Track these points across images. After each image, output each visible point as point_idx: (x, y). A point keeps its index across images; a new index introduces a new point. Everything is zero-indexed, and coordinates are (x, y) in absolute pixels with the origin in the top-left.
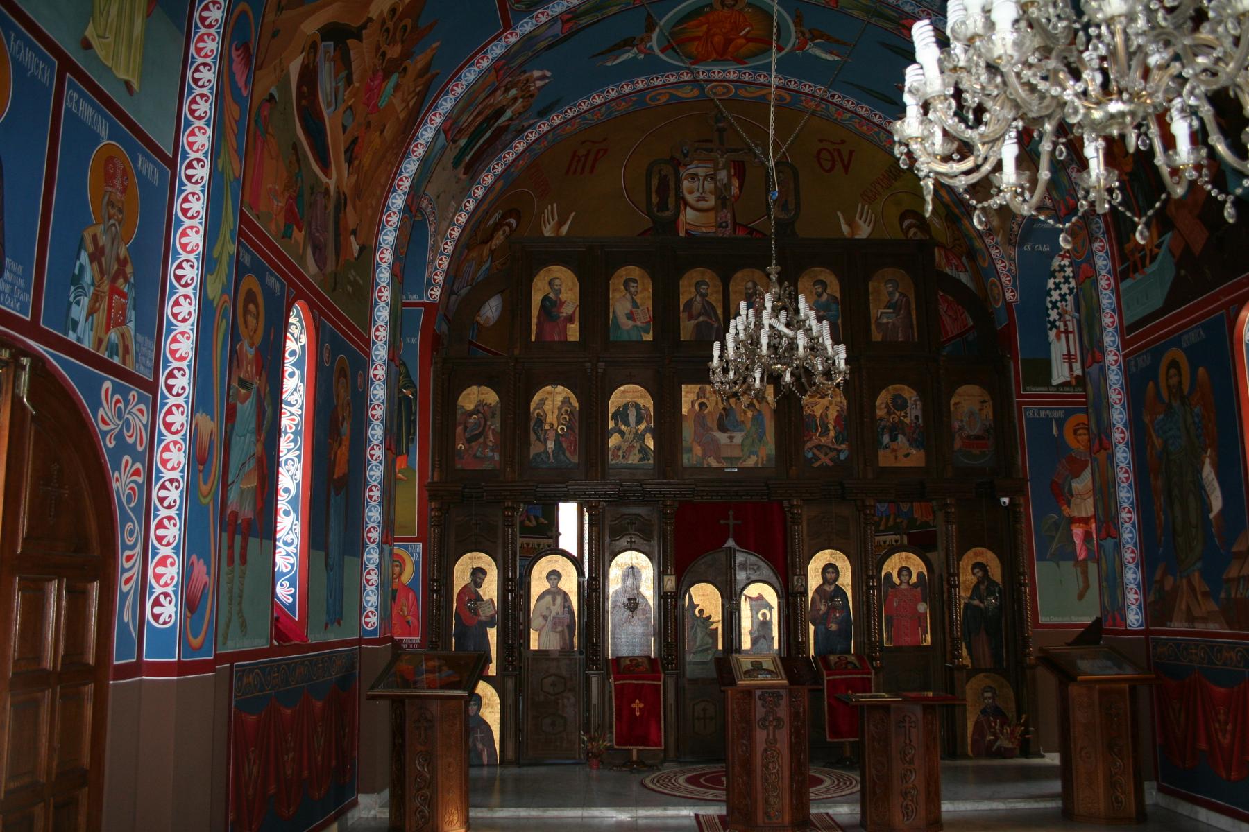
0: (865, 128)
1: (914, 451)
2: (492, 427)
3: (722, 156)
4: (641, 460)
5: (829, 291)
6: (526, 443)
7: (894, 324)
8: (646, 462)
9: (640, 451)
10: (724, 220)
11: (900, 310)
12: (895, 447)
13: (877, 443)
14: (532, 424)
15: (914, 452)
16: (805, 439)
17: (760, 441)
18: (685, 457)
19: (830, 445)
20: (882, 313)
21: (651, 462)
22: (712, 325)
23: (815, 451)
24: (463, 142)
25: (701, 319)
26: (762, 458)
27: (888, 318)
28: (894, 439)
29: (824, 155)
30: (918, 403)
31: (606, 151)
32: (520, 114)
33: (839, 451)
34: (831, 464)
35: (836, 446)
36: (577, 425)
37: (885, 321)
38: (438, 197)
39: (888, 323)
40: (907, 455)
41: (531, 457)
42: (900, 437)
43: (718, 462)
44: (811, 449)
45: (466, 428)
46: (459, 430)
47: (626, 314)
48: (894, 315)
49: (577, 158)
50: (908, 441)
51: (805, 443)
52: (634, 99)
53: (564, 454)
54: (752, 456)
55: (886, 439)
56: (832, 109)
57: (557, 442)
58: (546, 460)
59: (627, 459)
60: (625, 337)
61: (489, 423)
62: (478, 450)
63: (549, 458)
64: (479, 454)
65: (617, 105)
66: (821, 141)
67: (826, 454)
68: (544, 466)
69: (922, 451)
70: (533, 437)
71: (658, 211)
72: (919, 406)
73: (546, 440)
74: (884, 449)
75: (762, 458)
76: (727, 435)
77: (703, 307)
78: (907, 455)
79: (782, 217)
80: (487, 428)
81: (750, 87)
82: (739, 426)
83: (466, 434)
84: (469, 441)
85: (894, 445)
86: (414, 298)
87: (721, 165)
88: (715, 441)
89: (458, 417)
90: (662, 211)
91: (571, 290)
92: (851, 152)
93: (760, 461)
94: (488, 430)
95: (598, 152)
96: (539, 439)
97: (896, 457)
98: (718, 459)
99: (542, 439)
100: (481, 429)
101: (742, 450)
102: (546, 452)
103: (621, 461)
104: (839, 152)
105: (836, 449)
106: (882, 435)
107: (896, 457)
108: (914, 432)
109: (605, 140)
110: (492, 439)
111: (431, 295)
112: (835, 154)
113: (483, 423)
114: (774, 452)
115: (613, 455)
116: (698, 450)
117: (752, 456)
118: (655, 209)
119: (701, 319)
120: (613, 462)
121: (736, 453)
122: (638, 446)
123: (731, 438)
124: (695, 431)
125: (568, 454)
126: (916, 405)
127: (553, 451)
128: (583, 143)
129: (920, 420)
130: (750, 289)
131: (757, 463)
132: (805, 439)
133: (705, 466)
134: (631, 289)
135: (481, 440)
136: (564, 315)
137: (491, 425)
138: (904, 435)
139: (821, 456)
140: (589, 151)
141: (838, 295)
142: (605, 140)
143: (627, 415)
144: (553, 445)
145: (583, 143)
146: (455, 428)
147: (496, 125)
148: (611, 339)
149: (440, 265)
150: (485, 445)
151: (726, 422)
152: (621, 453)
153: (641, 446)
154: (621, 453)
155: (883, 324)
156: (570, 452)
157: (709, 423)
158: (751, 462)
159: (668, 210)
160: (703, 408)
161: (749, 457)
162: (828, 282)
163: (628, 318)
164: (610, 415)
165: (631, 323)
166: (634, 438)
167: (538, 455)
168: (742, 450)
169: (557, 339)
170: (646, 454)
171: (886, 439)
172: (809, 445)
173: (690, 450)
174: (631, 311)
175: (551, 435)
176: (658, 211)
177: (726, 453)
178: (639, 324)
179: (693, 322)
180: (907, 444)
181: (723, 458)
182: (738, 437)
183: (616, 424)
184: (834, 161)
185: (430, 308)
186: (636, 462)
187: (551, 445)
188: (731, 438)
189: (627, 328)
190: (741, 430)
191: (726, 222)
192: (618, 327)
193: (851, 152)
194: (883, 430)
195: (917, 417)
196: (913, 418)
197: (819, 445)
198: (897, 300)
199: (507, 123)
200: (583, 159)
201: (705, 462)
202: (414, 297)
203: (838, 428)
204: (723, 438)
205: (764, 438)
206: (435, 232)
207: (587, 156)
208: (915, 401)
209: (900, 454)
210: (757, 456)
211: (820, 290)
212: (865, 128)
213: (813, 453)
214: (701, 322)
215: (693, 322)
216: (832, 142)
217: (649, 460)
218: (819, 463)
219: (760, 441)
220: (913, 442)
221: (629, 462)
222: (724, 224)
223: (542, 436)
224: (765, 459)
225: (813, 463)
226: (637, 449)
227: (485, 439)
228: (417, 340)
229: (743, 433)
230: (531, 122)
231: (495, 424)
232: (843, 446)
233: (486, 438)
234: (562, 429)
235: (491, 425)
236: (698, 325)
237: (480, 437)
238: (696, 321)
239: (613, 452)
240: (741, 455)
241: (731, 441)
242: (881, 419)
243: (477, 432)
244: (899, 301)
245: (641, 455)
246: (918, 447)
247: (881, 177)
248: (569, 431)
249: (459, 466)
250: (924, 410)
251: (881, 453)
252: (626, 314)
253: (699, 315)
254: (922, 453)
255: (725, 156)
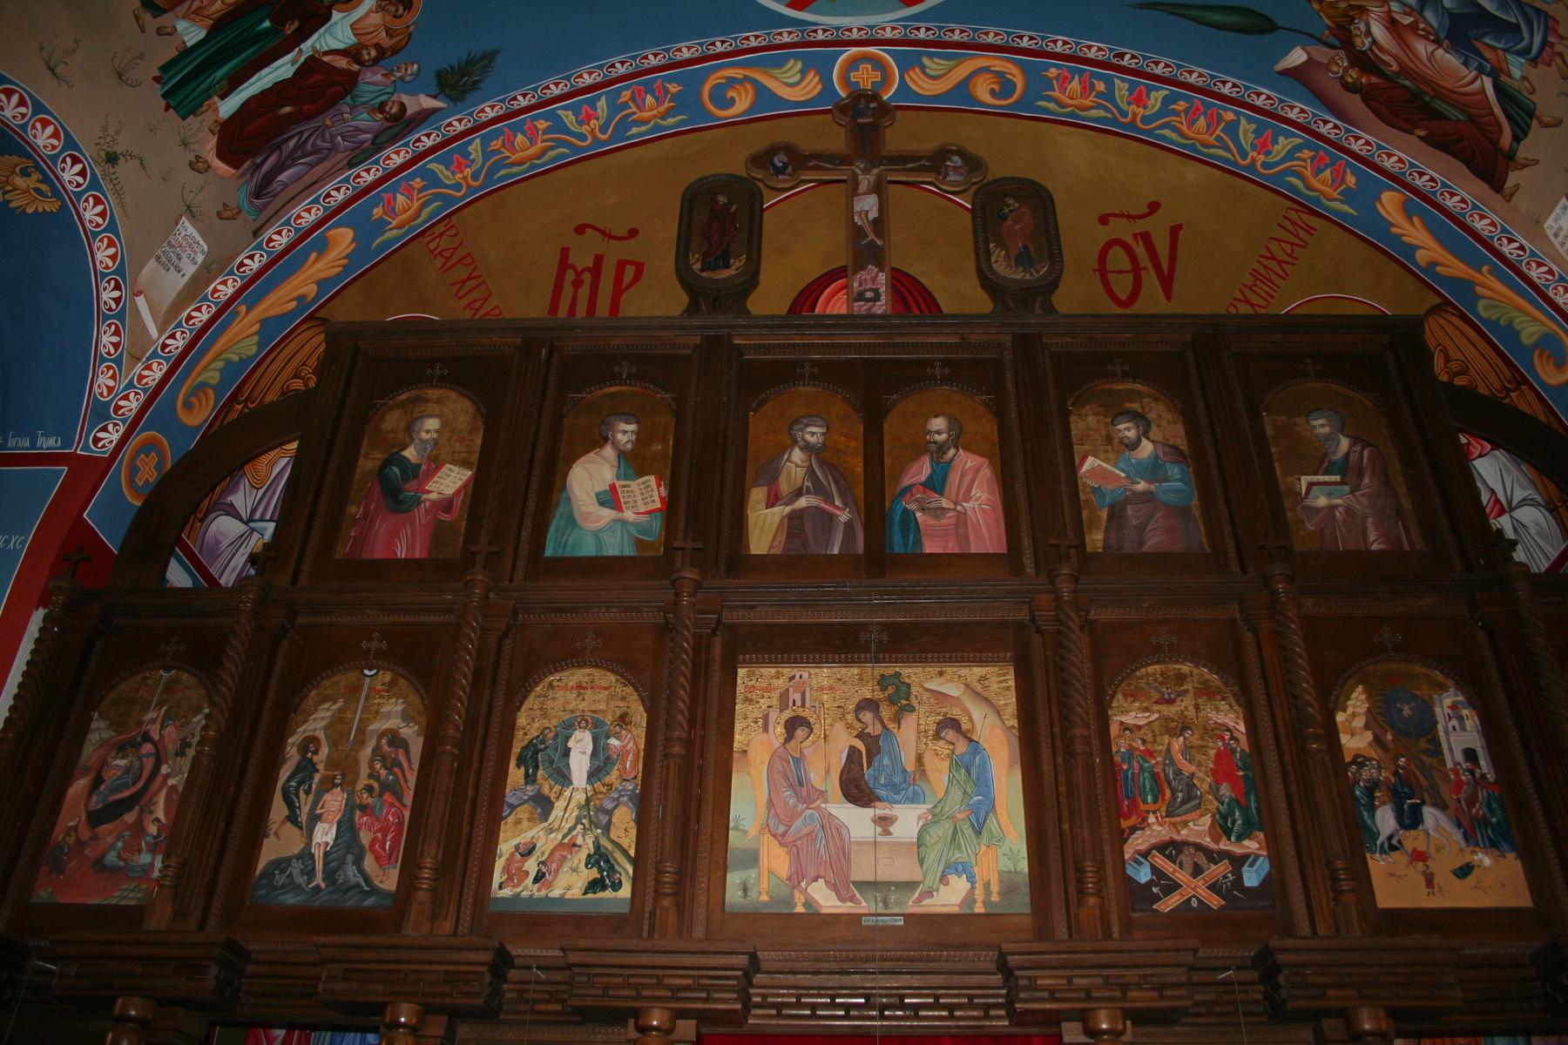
0: (1202, 122)
1: (1484, 859)
2: (171, 782)
3: (866, 171)
4: (595, 885)
5: (1155, 433)
6: (257, 829)
7: (1349, 510)
8: (608, 894)
9: (591, 861)
10: (869, 286)
11: (1360, 474)
12: (1421, 846)
13: (1360, 838)
14: (285, 773)
15: (1487, 861)
16: (1125, 824)
17: (979, 833)
18: (734, 879)
19: (1207, 841)
20: (1311, 485)
21: (625, 892)
22: (831, 517)
23: (1160, 860)
24: (192, 33)
25: (802, 502)
26: (987, 886)
27: (1329, 495)
28: (1408, 819)
29: (1118, 258)
30: (1465, 712)
31: (640, 268)
32: (382, 53)
33: (1238, 862)
34: (1215, 902)
35: (1224, 845)
36: (412, 780)
37: (1322, 502)
38: (112, 159)
39: (1332, 508)
40: (1464, 871)
41: (262, 864)
42: (1429, 814)
43: (841, 899)
44: (1146, 854)
45: (98, 781)
46: (79, 786)
47: (597, 495)
48: (1347, 488)
49: (570, 276)
50: (1459, 825)
51: (1121, 837)
52: (674, 88)
53: (358, 863)
54: (952, 878)
55: (1385, 820)
56: (1121, 87)
57: (347, 828)
58: (300, 880)
59: (549, 885)
60: (588, 549)
61: (164, 769)
62: (112, 846)
63: (310, 874)
64: (111, 858)
65: (632, 98)
66: (1104, 220)
67: (1197, 871)
68: (290, 899)
69: (1511, 856)
70: (278, 809)
71: (702, 270)
72: (1471, 720)
73: (315, 818)
74: (1382, 851)
75: (987, 886)
76: (868, 813)
77: (810, 472)
78: (1464, 871)
79: (1018, 277)
80: (158, 781)
81: (931, 56)
82: (908, 786)
83: (95, 798)
84: (96, 819)
85: (1413, 840)
86: (49, 444)
87: (863, 186)
88: (832, 828)
89: (88, 750)
90: (714, 270)
91: (462, 440)
92: (1175, 230)
93: (979, 894)
94: (160, 789)
95: (622, 264)
96: (293, 818)
97: (1430, 881)
98: (840, 888)
99: (303, 818)
100: (140, 784)
101: (921, 861)
102: (306, 856)
103: (528, 889)
104: (1146, 238)
105: (1226, 855)
106: (1372, 809)
107: (1430, 881)
108: (1472, 801)
109: (633, 233)
110: (160, 814)
111: (96, 440)
112: (1140, 250)
113: (149, 764)
114: (1023, 865)
115: (506, 869)
116: (776, 860)
117: (952, 878)
118: (697, 266)
119: (802, 502)
120: (507, 892)
121: (900, 869)
122: (587, 845)
123: (884, 822)
124: (770, 801)
125: (369, 863)
126: (1461, 719)
127: (326, 854)
128: (580, 229)
129: (1482, 763)
130: (939, 432)
131: (969, 899)
132: (1125, 824)
133: (800, 909)
134: (620, 436)
135: (130, 818)
136: (434, 496)
137: (168, 776)
138: (1442, 806)
139: (1182, 876)
140: (599, 260)
141: (1184, 448)
142: (633, 233)
143: (567, 753)
144: (330, 838)
145: (580, 229)
146: (66, 783)
147: (307, 47)
148: (548, 553)
149: (141, 377)
150: (138, 828)
151: (868, 773)
152: (531, 866)
153: (598, 846)
154: (531, 866)
155: (1318, 510)
156: (378, 859)
157: (816, 777)
158: (950, 897)
159: (727, 266)
160: (800, 732)
161: (944, 880)
162: (1152, 416)
163: (602, 503)
164: (516, 750)
165: (608, 514)
166: (578, 821)
167: (281, 864)
168: (921, 861)
169: (401, 553)
170: (612, 869)
171: (1385, 820)
172: (1138, 842)
173: (752, 859)
174: (613, 487)
175: (335, 802)
176: (702, 270)
177: (862, 870)
178: (629, 515)
179: (780, 511)
180: (1458, 836)
181: (857, 884)
182: (908, 820)
183: (530, 779)
184: (1137, 270)
185: (89, 472)
186: (576, 892)
187: (325, 834)
188: (884, 822)
189: (594, 526)
190: (915, 799)
191: (876, 291)
192: (572, 522)
193: (1175, 230)
194: (1370, 791)
195: (1470, 754)
196: (1459, 757)
197: (1172, 843)
198: (1347, 454)
199: (342, 63)
200: (587, 277)
201: (799, 898)
202: (51, 442)
203: (1225, 790)
204: (857, 821)
205: (992, 823)
206: (120, 271)
207: (596, 270)
208: (1453, 707)
209: (1442, 866)
210: (971, 879)
211: (1132, 434)
212: (1202, 122)
213: (1154, 870)
214: (803, 510)
215: (780, 511)
216: (1129, 217)
217: (617, 886)
218: (1168, 904)
219: (979, 833)
220: (1472, 830)
221: (556, 893)
222: (869, 295)
223: (306, 809)
224: (995, 888)
225: (1157, 898)
226: (583, 855)
227: (142, 811)
228: (23, 543)
229: (922, 809)
230: (428, 103)
231: (176, 774)
232: (1251, 845)
233: (147, 810)
234: (370, 789)
235: (168, 776)
236: (795, 519)
237: (130, 809)
238: (788, 509)
239: (510, 860)
240: (916, 875)
241: (887, 833)
242: (1360, 761)
243: (126, 793)
244: (1353, 457)
245: (594, 874)
246: (1494, 845)
247: (1249, 280)
248: (387, 797)
249: (43, 895)
250: (1489, 729)
251: (1377, 865)
252: (597, 495)
253: (799, 493)
254: (1512, 865)
255: (875, 171)
